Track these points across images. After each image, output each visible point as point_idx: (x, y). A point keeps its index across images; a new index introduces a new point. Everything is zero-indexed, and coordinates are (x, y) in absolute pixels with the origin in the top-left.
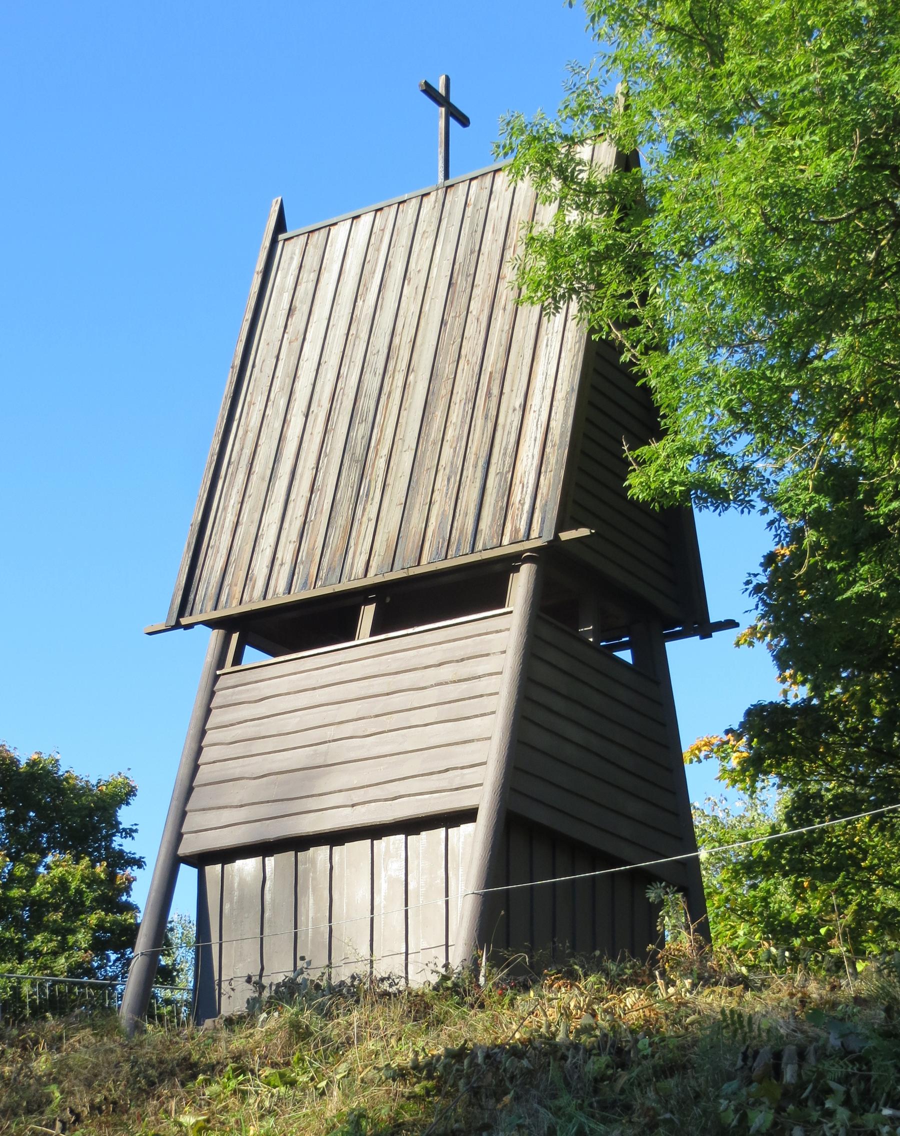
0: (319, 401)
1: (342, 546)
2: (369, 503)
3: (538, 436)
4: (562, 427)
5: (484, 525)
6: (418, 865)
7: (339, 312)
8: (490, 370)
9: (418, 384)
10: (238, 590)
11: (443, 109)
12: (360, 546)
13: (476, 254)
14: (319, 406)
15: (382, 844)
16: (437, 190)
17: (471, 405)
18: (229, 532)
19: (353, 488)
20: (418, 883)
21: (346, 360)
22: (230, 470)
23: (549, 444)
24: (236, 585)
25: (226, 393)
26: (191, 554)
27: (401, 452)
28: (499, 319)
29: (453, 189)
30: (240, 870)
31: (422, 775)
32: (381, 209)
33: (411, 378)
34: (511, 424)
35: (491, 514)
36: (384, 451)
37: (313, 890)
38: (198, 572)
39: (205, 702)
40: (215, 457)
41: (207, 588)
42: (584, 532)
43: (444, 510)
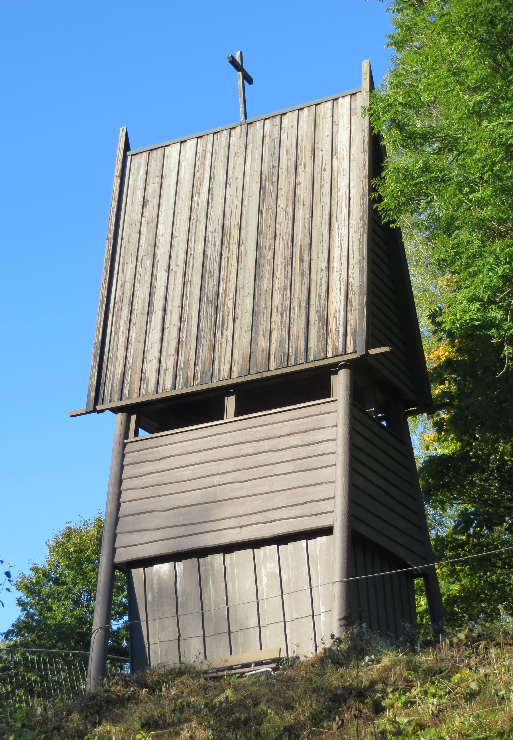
0: (176, 262)
1: (209, 358)
2: (225, 329)
3: (342, 287)
4: (359, 282)
5: (312, 344)
7: (182, 204)
10: (136, 387)
11: (241, 73)
13: (277, 168)
14: (176, 265)
15: (261, 552)
16: (241, 125)
17: (290, 267)
20: (289, 576)
21: (192, 236)
23: (350, 292)
24: (134, 384)
26: (97, 363)
27: (243, 296)
28: (301, 211)
29: (252, 125)
30: (158, 572)
31: (289, 506)
32: (201, 137)
33: (242, 248)
34: (321, 279)
36: (231, 296)
38: (103, 375)
39: (119, 460)
40: (105, 299)
41: (112, 386)
42: (385, 349)
43: (281, 335)
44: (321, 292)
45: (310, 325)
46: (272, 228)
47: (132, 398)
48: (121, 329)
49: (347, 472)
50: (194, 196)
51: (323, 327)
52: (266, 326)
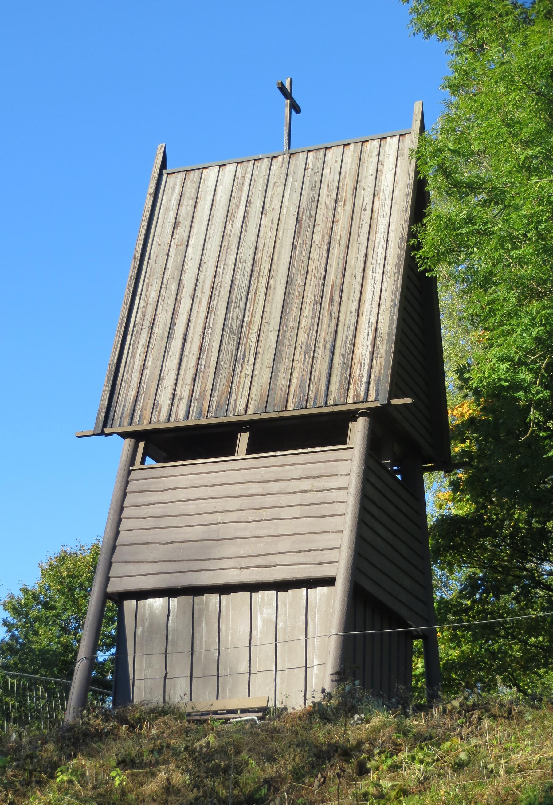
0: (202, 289)
1: (226, 391)
2: (246, 364)
3: (370, 332)
4: (389, 329)
5: (334, 387)
6: (286, 611)
7: (214, 229)
8: (331, 283)
9: (277, 286)
10: (147, 413)
11: (289, 101)
12: (240, 393)
13: (316, 203)
14: (202, 292)
15: (259, 596)
16: (284, 155)
17: (318, 306)
18: (138, 373)
19: (232, 352)
20: (285, 624)
21: (221, 264)
22: (136, 329)
23: (378, 338)
24: (146, 410)
25: (130, 275)
26: (110, 385)
27: (268, 331)
28: (336, 250)
29: (295, 156)
30: (150, 606)
31: (292, 552)
32: (241, 162)
33: (272, 281)
34: (350, 321)
35: (338, 381)
36: (255, 330)
37: (206, 624)
38: (115, 398)
39: (123, 487)
40: (125, 319)
41: (123, 410)
43: (303, 375)
44: (347, 335)
45: (333, 368)
46: (305, 264)
47: (142, 424)
48: (139, 352)
49: (356, 523)
50: (228, 223)
51: (346, 371)
52: (288, 364)
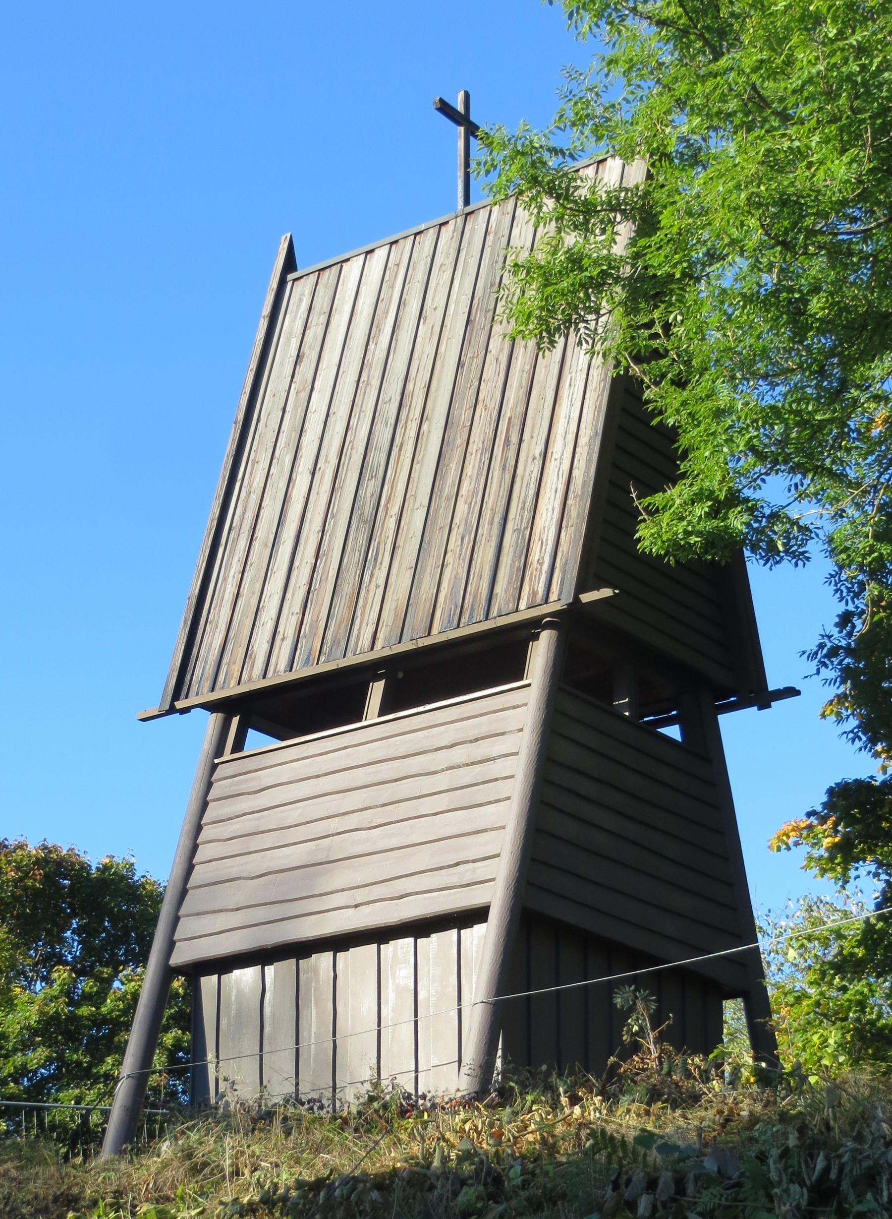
0: (327, 456)
4: (584, 475)
5: (499, 589)
6: (429, 971)
8: (508, 415)
9: (432, 433)
10: (237, 668)
11: (462, 129)
14: (326, 462)
16: (456, 217)
17: (488, 455)
19: (360, 551)
22: (231, 537)
23: (571, 495)
24: (234, 663)
25: (228, 451)
26: (187, 630)
27: (413, 510)
28: (520, 358)
29: (473, 216)
32: (396, 242)
33: (425, 427)
34: (530, 474)
35: (507, 575)
36: (395, 510)
37: (316, 1002)
38: (195, 650)
40: (215, 522)
42: (606, 593)
43: (457, 573)
44: (526, 497)
45: (502, 554)
46: (473, 391)
47: (228, 687)
48: (233, 571)
49: (526, 811)
50: (371, 343)
51: (520, 557)
52: (438, 558)
